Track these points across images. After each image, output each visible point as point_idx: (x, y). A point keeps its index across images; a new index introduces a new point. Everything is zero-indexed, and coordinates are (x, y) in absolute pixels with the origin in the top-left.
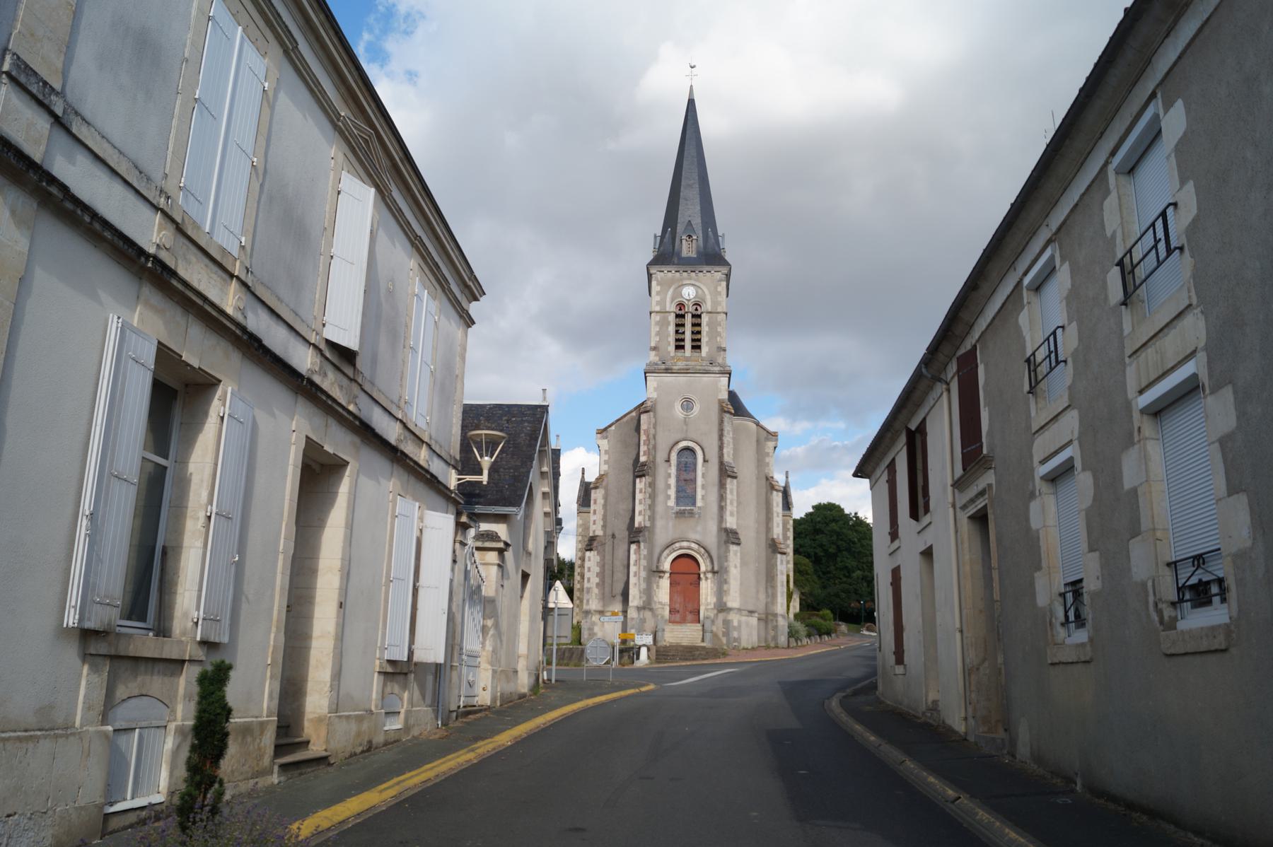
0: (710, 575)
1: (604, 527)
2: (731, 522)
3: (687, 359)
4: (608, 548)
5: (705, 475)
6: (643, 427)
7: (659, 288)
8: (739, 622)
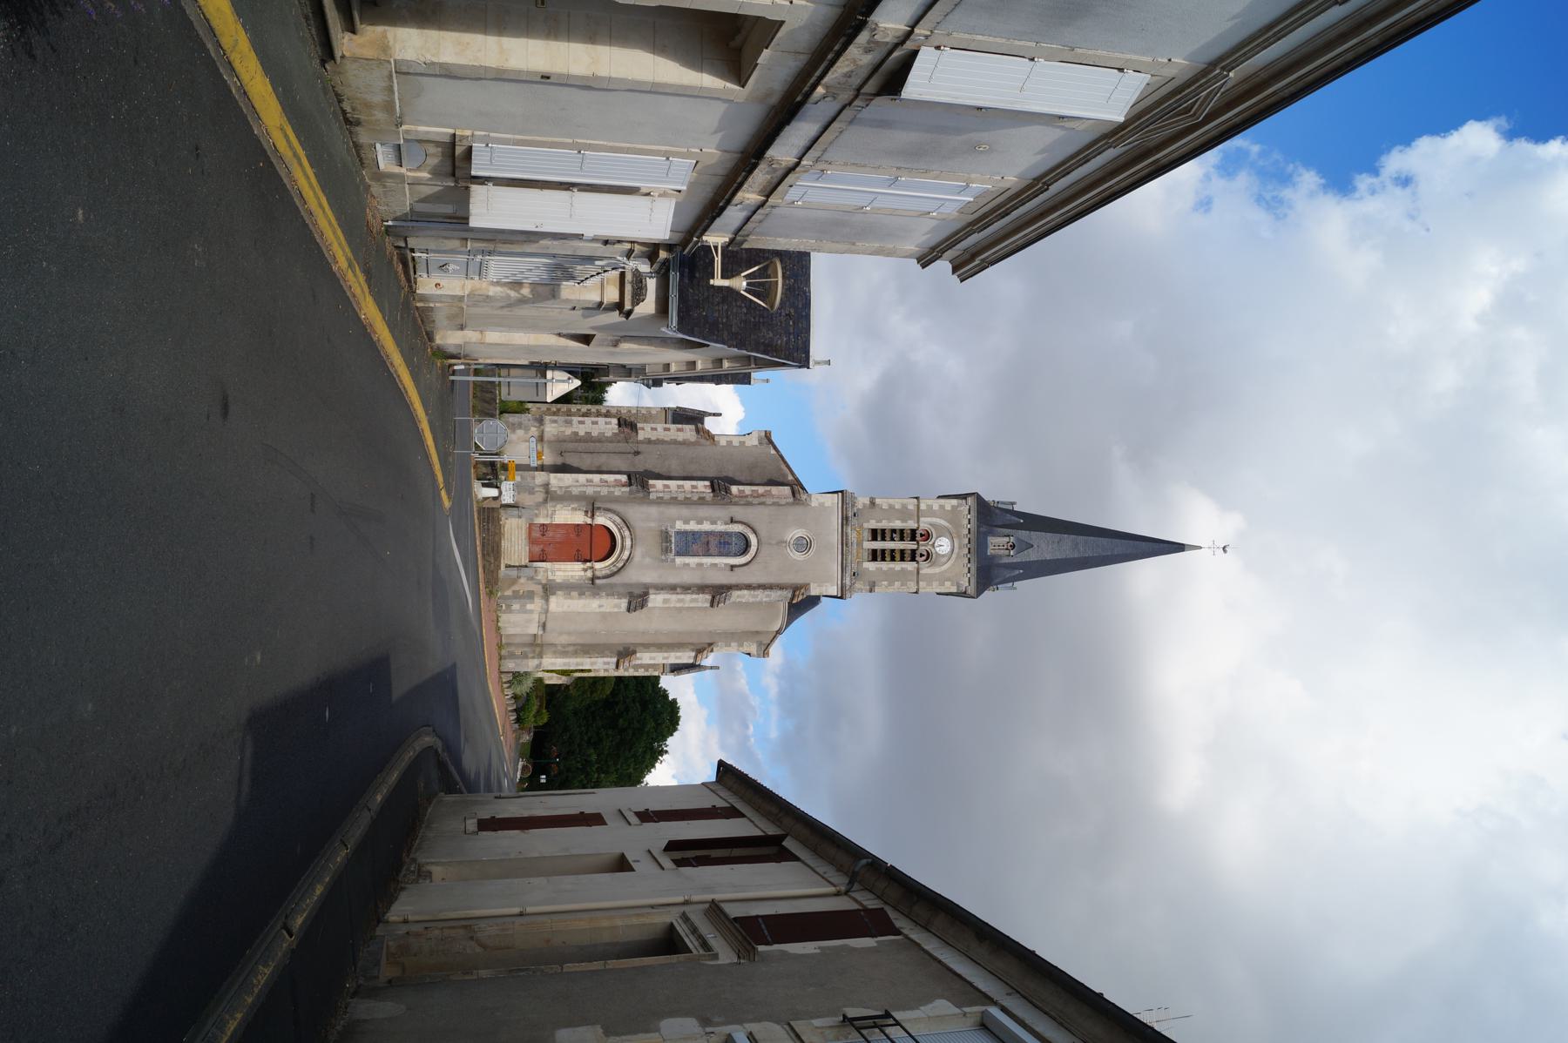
0: (589, 574)
1: (649, 441)
2: (656, 600)
3: (860, 544)
4: (622, 446)
5: (715, 567)
6: (775, 490)
7: (948, 508)
8: (531, 612)
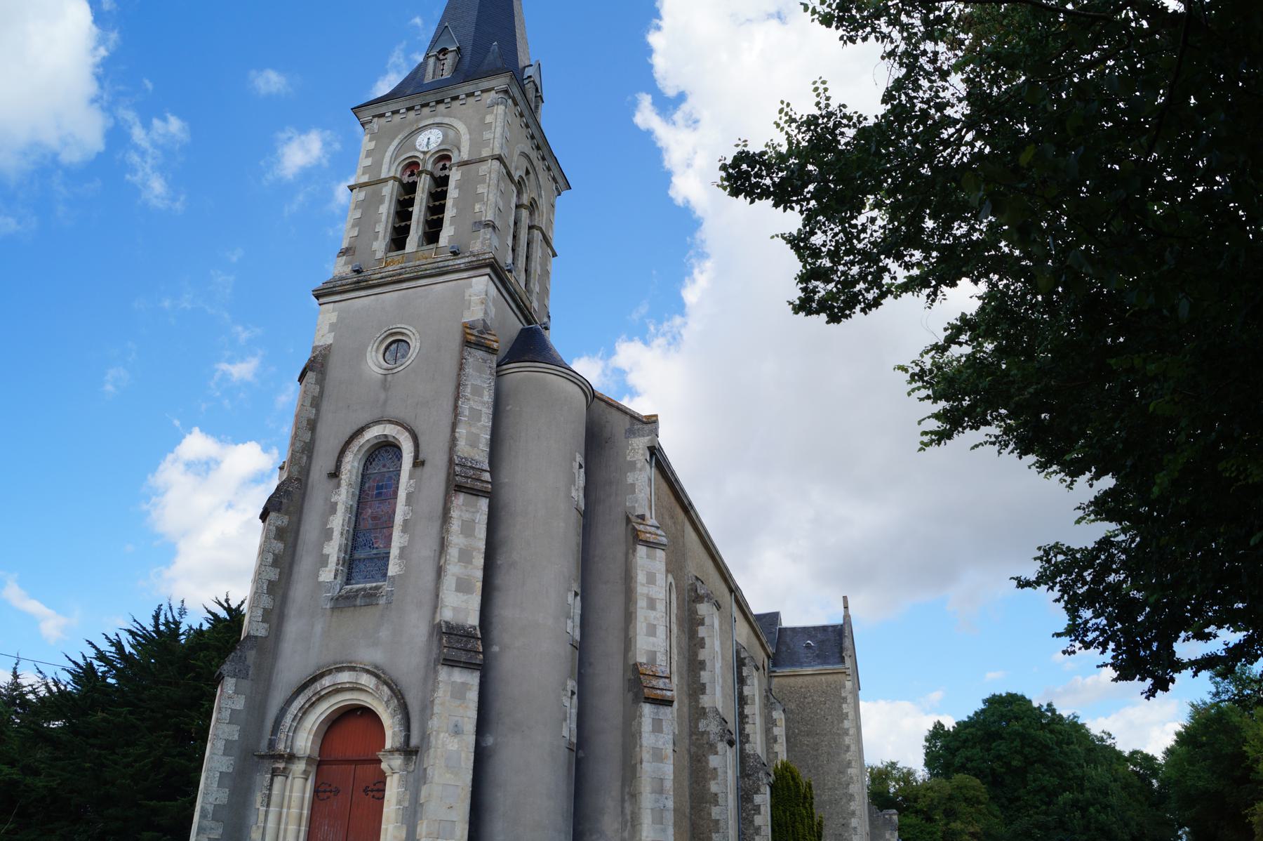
5: (413, 493)
7: (372, 145)
